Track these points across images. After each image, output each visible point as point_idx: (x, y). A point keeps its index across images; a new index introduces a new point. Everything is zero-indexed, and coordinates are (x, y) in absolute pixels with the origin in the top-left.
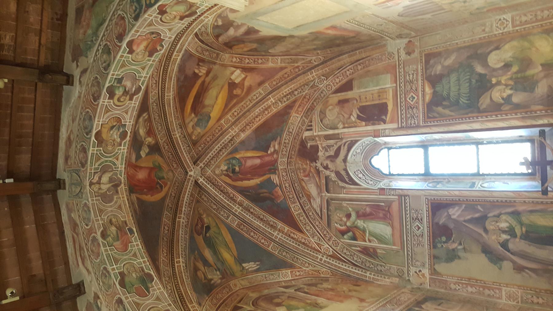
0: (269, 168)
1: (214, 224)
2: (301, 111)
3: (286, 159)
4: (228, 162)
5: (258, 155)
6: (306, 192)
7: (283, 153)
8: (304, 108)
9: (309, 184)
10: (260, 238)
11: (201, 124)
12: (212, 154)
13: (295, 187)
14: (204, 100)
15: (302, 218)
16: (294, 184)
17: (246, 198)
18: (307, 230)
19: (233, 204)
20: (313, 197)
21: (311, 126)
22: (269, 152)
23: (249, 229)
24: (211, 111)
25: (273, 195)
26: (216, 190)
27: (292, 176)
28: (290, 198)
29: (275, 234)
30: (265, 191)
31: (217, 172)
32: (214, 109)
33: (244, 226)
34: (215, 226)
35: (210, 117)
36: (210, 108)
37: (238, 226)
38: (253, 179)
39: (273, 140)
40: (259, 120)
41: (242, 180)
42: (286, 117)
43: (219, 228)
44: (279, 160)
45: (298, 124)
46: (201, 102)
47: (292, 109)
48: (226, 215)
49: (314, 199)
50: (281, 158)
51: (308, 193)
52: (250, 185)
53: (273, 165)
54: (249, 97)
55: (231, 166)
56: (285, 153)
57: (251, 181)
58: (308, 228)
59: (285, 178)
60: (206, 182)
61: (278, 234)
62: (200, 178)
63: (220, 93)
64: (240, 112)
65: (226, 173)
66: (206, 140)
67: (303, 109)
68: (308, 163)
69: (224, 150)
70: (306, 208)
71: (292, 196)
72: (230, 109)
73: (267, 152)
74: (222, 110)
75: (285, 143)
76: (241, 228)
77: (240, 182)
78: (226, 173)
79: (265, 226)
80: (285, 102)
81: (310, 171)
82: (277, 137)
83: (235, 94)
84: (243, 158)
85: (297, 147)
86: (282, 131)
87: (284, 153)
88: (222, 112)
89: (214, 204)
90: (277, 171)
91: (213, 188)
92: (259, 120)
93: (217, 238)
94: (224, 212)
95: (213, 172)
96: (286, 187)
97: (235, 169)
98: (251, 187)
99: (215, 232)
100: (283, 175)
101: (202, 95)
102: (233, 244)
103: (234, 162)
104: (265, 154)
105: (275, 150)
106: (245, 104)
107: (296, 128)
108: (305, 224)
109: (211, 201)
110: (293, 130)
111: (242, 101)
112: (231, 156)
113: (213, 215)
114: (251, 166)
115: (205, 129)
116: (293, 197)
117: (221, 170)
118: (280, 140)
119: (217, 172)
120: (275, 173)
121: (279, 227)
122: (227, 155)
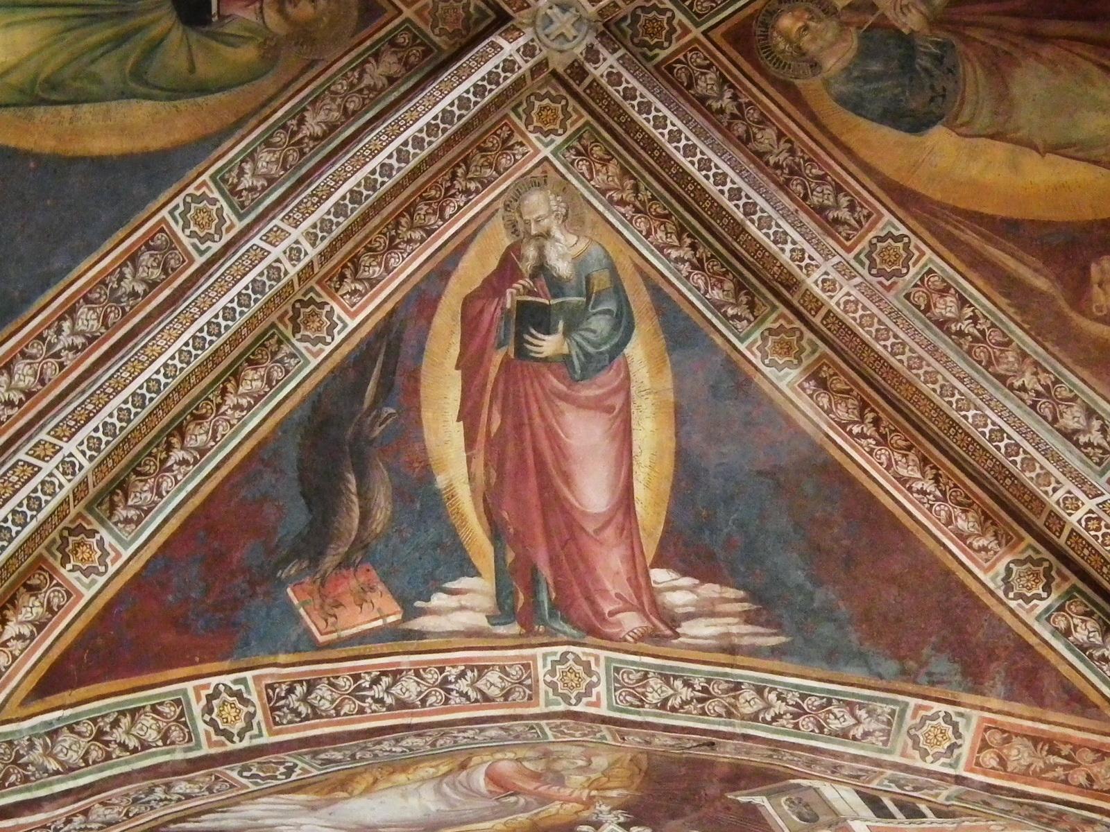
0: (545, 572)
1: (206, 69)
2: (1003, 762)
3: (604, 711)
4: (601, 280)
5: (640, 491)
6: (369, 779)
7: (655, 682)
8: (1037, 777)
9: (438, 790)
10: (51, 369)
11: (876, 67)
12: (675, 137)
13: (397, 741)
14: (1047, 52)
15: (152, 735)
16: (420, 735)
17: (339, 372)
18: (54, 734)
19: (325, 225)
20: (334, 801)
21: (912, 813)
22: (660, 576)
23: (126, 317)
24: (965, 131)
25: (345, 563)
26: (431, 129)
27: (482, 730)
28: (311, 686)
29: (70, 447)
30: (381, 516)
31: (538, 204)
32: (982, 142)
33: (152, 285)
34: (192, 69)
35: (917, 124)
36: (984, 121)
37: (160, 239)
38: (470, 442)
39: (754, 595)
40: (903, 481)
41: (470, 366)
42: (941, 665)
43: (176, 92)
44: (599, 657)
45: (895, 766)
46: (1032, 35)
47: (1009, 697)
48: (247, 181)
49: (314, 809)
50: (615, 670)
51: (361, 787)
52: (427, 415)
53: (562, 608)
54: (1072, 381)
55: (575, 299)
56: (653, 698)
57: (455, 432)
58: (70, 748)
59: (463, 685)
60: (492, 78)
61: (69, 467)
62: (521, 41)
63: (1096, 162)
64: (961, 334)
65: (527, 266)
66: (764, 121)
67: (1026, 774)
68: (614, 794)
69: (687, 253)
70: (234, 774)
71: (325, 705)
72: (977, 263)
73: (659, 562)
74: (962, 205)
75: (737, 687)
76: (146, 257)
77: (455, 350)
78: (527, 266)
79: (139, 400)
80: (1067, 633)
81: (545, 800)
82: (776, 625)
83: (1094, 269)
84: (625, 386)
85: (727, 754)
86: (833, 657)
87: (655, 690)
88: (955, 210)
89: (332, 128)
90: (515, 629)
91: (447, 116)
92: (903, 481)
93: (121, 40)
94: (271, 180)
95: (534, 182)
96: (397, 675)
97: (548, 333)
98: (418, 423)
99: (156, 45)
100: (482, 670)
101: (1080, 28)
102: (47, 145)
103: (600, 324)
104: (650, 550)
105: (673, 621)
106: (1024, 355)
107: (856, 758)
108: (99, 736)
109: (356, 114)
110: (843, 734)
111: (1038, 335)
112: (640, 300)
113: (268, 85)
114: (560, 451)
115: (842, 101)
116: (316, 713)
117: (547, 235)
118: (754, 651)
119: (538, 204)
120: (504, 610)
121: (103, 533)
122: (646, 278)
